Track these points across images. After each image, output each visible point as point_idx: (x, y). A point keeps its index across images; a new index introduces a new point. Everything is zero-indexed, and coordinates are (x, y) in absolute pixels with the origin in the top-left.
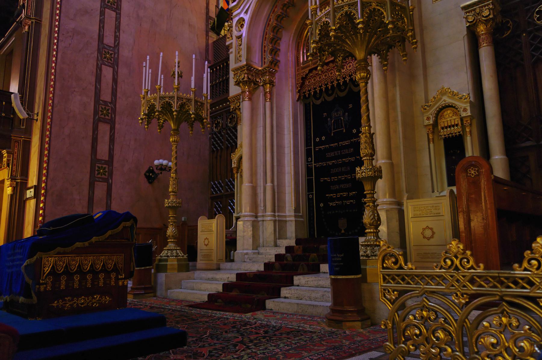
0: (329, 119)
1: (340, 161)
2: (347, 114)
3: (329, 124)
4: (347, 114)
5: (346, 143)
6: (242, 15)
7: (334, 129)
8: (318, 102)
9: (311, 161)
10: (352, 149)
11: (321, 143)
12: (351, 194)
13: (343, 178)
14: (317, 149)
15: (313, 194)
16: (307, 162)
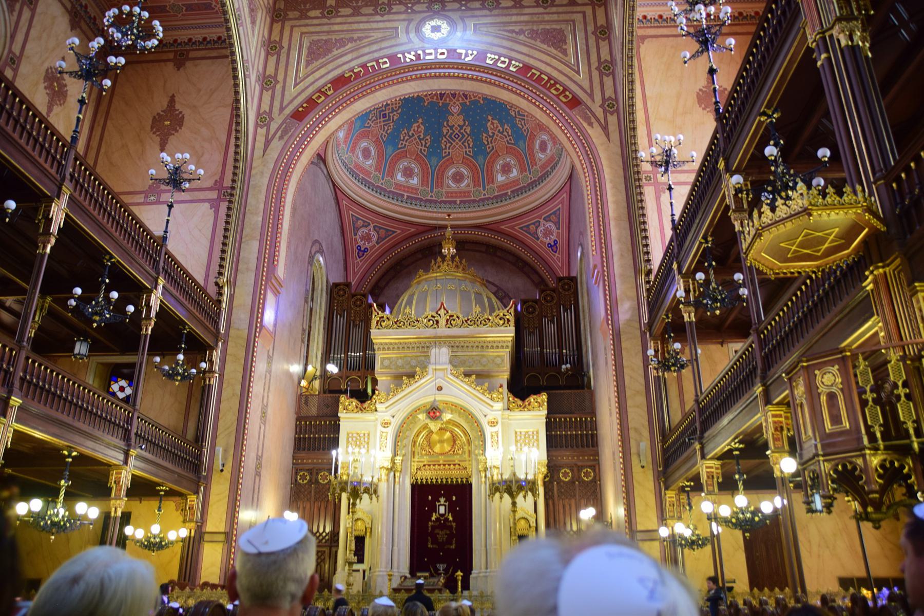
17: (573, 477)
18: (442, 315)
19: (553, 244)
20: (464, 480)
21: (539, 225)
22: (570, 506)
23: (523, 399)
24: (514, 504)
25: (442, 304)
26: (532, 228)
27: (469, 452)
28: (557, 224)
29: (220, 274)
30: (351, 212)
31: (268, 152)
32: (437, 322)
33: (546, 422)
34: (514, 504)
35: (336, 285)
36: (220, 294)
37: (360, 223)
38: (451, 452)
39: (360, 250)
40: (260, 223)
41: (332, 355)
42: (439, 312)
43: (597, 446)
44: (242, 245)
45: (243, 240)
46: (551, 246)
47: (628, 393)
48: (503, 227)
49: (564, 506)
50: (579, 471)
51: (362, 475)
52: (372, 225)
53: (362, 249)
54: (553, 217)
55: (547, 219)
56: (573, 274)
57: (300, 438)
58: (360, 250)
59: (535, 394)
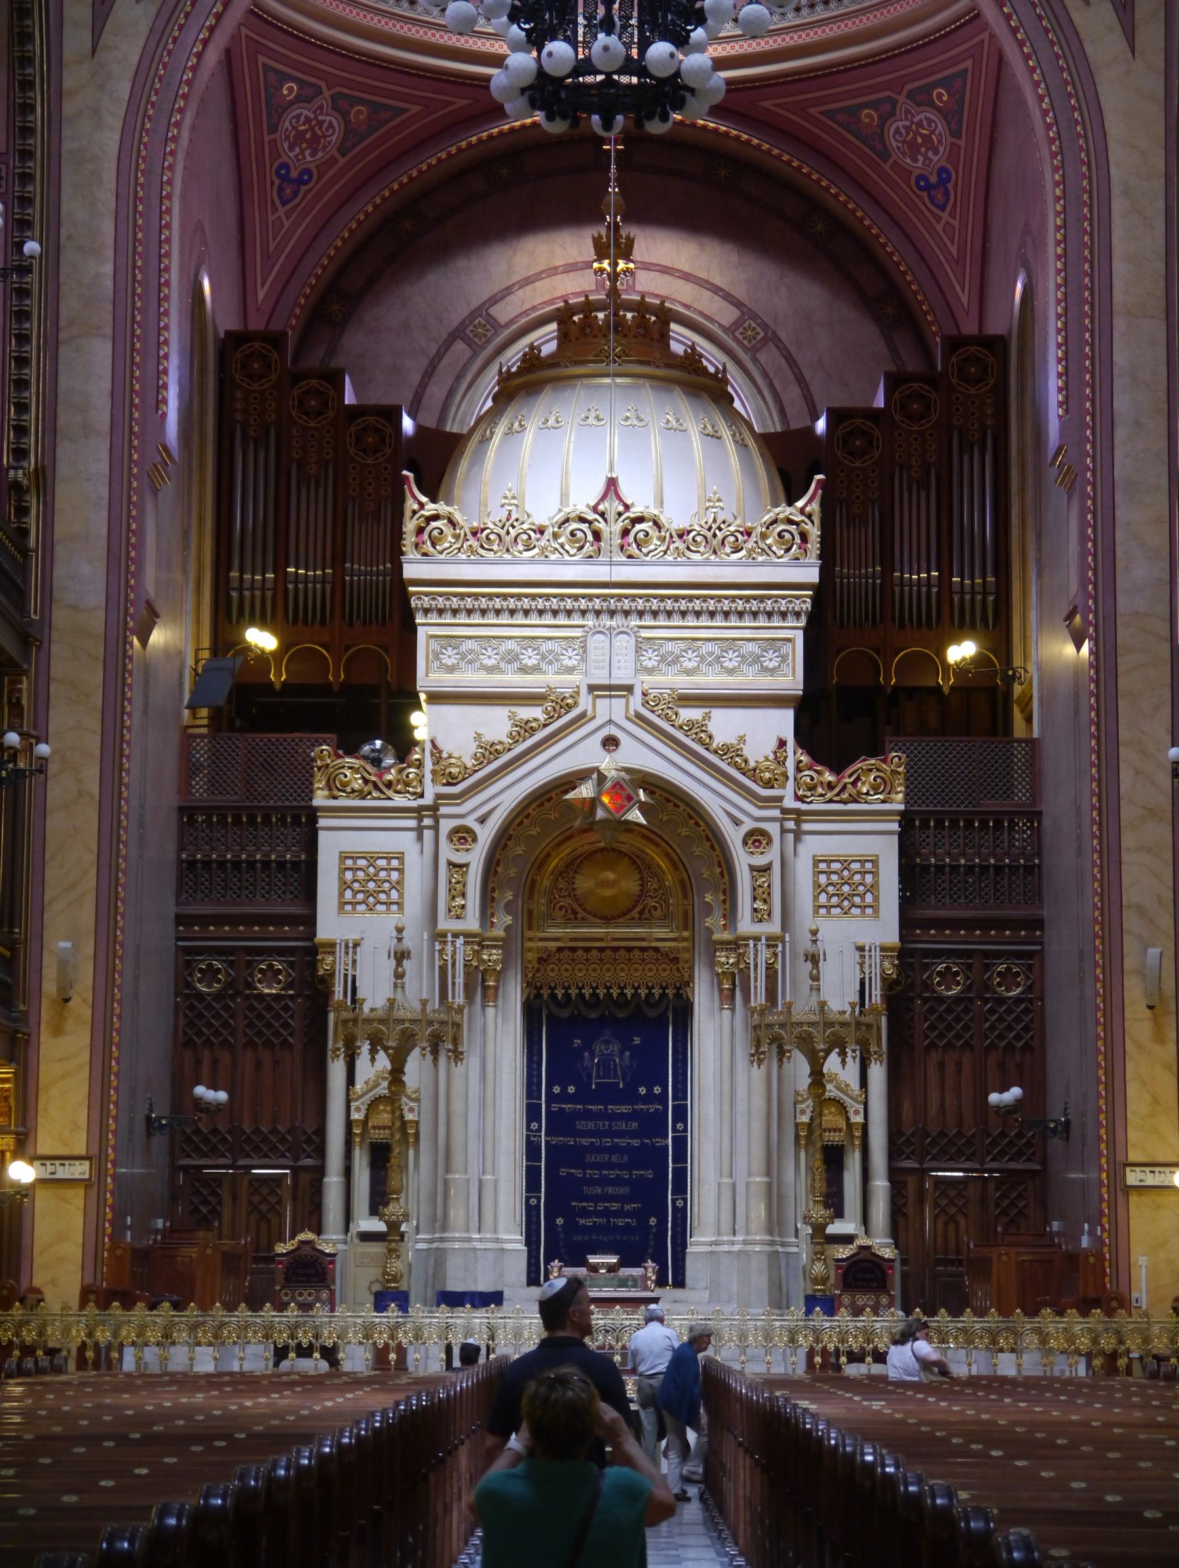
0: (586, 1054)
1: (608, 1142)
2: (627, 1053)
3: (587, 1063)
4: (627, 1053)
5: (624, 1109)
6: (470, 822)
7: (598, 1077)
8: (565, 1014)
9: (539, 1130)
10: (635, 1124)
11: (564, 1097)
12: (627, 1207)
13: (613, 1174)
14: (555, 1107)
15: (539, 1199)
16: (528, 1128)
17: (968, 988)
18: (611, 516)
19: (933, 179)
20: (670, 992)
21: (892, 114)
22: (959, 1064)
23: (837, 769)
24: (818, 1077)
25: (612, 483)
26: (868, 116)
27: (686, 912)
28: (951, 115)
29: (20, 454)
30: (261, 59)
31: (106, 38)
32: (597, 536)
33: (902, 836)
34: (818, 1077)
35: (234, 341)
36: (23, 511)
37: (289, 90)
38: (635, 913)
39: (285, 179)
40: (109, 283)
41: (234, 574)
42: (601, 507)
43: (1041, 900)
44: (63, 350)
45: (63, 335)
46: (929, 187)
47: (1126, 812)
48: (767, 104)
49: (941, 1066)
50: (987, 967)
51: (424, 1003)
52: (327, 94)
53: (294, 174)
54: (941, 95)
55: (921, 98)
56: (995, 327)
57: (192, 864)
58: (285, 179)
59: (873, 755)
